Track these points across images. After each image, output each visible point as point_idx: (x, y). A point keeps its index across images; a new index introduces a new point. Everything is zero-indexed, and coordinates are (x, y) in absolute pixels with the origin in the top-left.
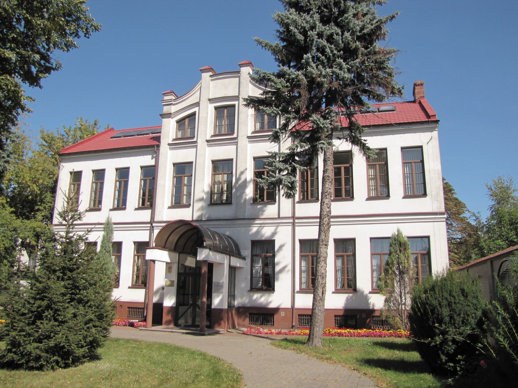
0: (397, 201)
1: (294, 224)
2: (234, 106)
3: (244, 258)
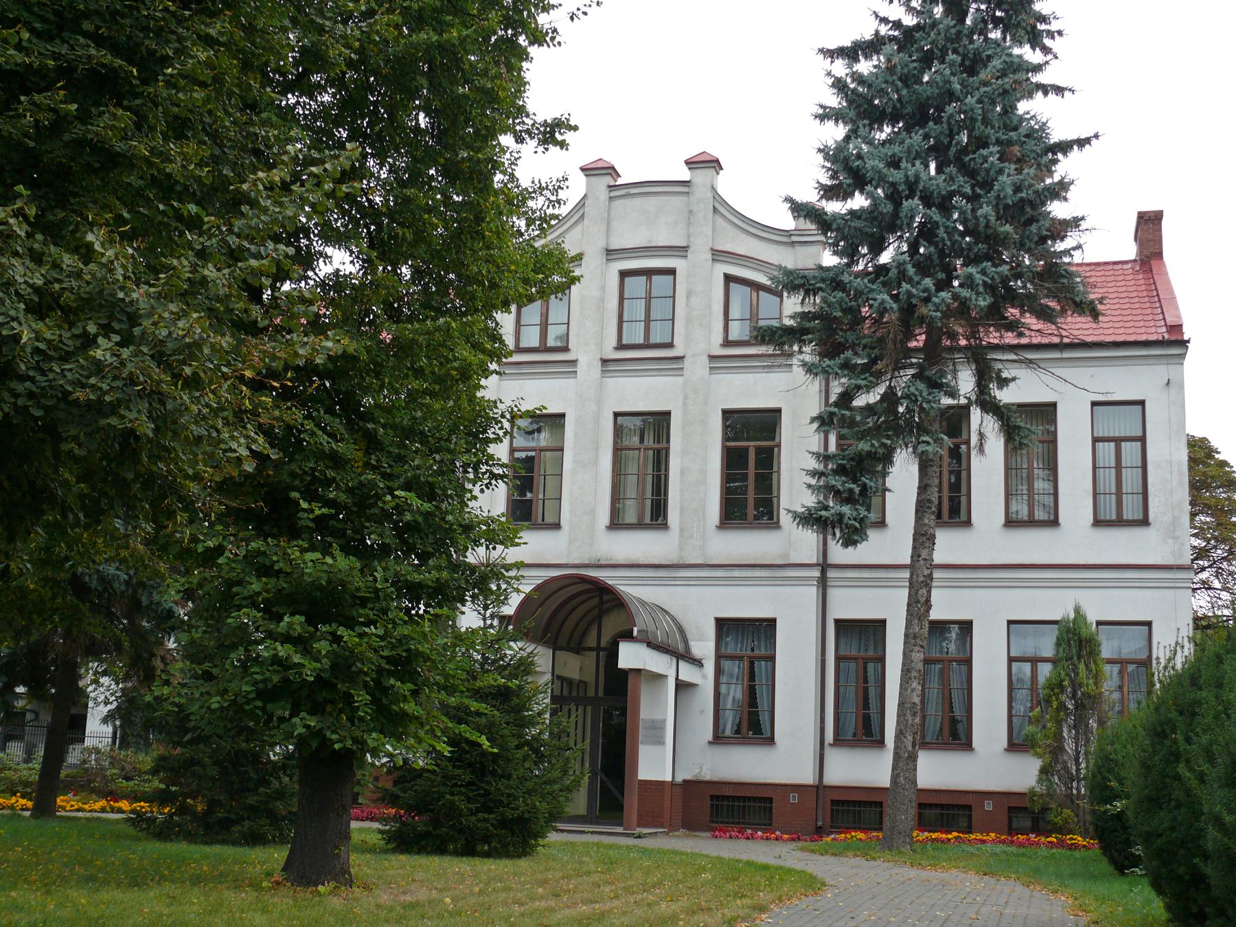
0: (1076, 537)
1: (823, 583)
2: (672, 272)
3: (698, 663)
